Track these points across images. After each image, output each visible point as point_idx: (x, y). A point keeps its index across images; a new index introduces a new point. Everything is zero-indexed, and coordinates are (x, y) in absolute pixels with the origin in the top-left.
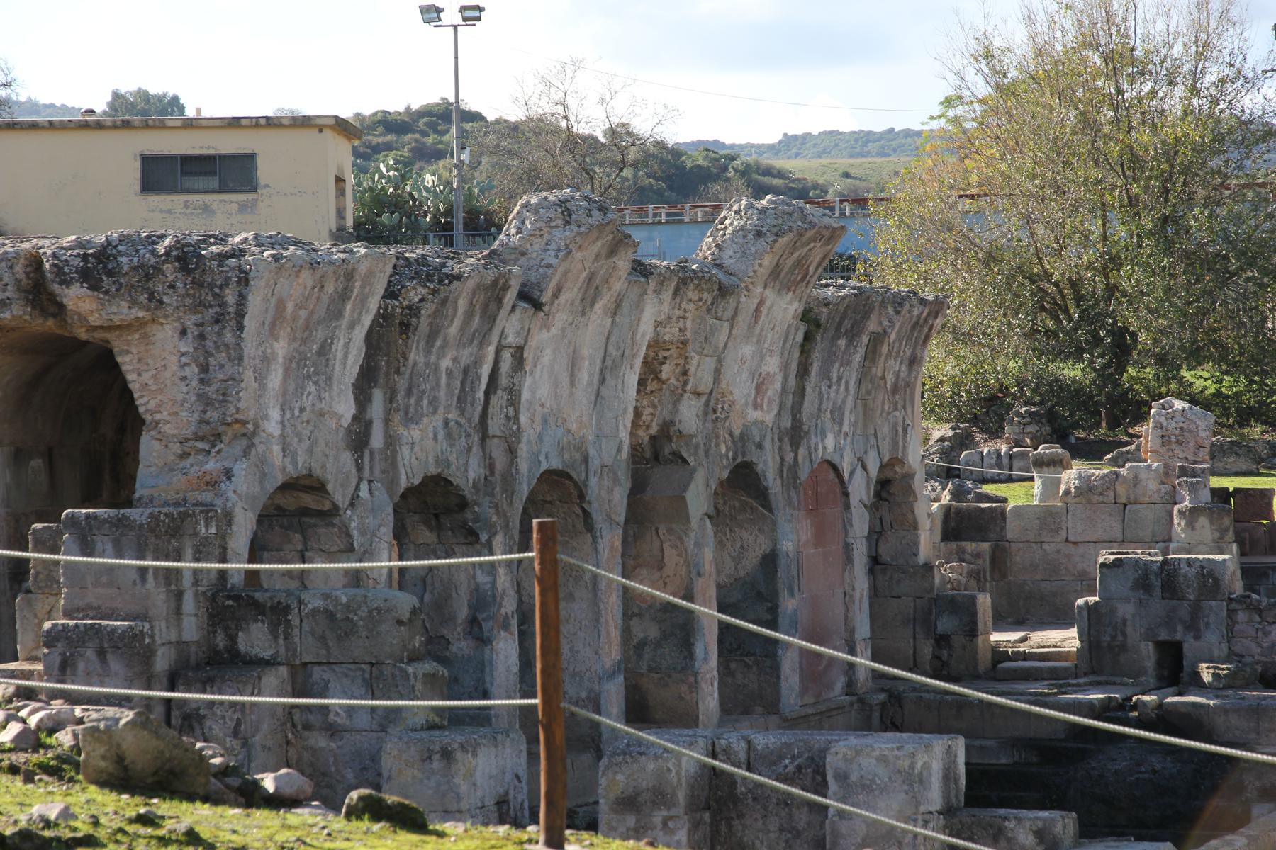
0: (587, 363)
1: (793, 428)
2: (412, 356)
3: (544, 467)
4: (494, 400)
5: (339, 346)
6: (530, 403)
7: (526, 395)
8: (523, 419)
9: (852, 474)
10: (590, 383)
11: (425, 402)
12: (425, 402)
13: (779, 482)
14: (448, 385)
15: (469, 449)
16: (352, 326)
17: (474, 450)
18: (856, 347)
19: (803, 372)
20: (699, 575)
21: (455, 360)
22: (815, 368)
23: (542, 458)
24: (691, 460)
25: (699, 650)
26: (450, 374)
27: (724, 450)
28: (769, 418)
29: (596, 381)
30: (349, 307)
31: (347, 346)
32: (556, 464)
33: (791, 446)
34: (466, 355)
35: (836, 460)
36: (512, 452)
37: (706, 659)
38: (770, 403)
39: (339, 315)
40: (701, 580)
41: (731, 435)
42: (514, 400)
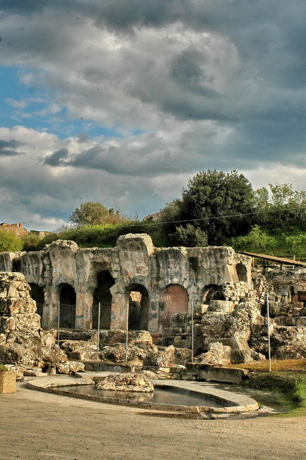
0: (71, 266)
1: (157, 277)
2: (22, 266)
3: (60, 282)
4: (45, 272)
5: (6, 265)
6: (55, 273)
7: (54, 271)
8: (53, 275)
9: (190, 287)
10: (73, 269)
11: (27, 273)
12: (27, 273)
13: (150, 288)
14: (32, 270)
15: (39, 279)
16: (7, 263)
17: (40, 279)
18: (180, 260)
19: (158, 266)
20: (113, 303)
21: (33, 267)
22: (161, 265)
23: (60, 281)
24: (116, 282)
25: (112, 316)
26: (32, 269)
27: (125, 281)
28: (146, 274)
29: (75, 269)
30: (4, 260)
31: (7, 265)
32: (63, 282)
33: (156, 280)
34: (35, 266)
35: (180, 283)
36: (51, 281)
37: (115, 318)
38: (144, 272)
39: (3, 261)
40: (113, 304)
41: (129, 278)
42: (51, 272)
